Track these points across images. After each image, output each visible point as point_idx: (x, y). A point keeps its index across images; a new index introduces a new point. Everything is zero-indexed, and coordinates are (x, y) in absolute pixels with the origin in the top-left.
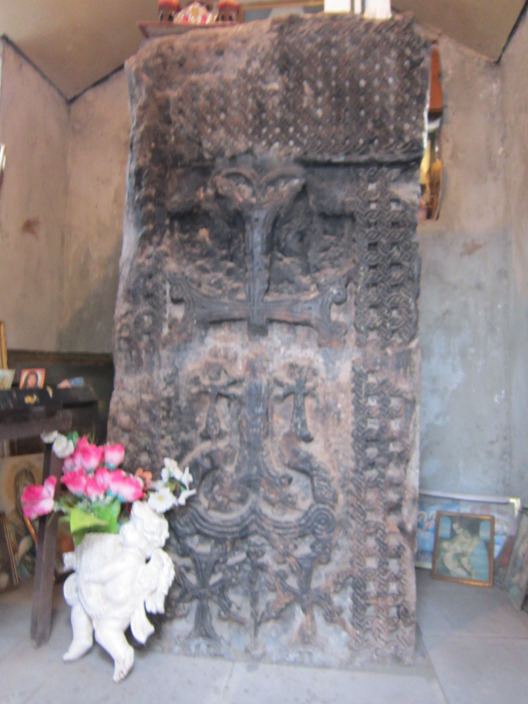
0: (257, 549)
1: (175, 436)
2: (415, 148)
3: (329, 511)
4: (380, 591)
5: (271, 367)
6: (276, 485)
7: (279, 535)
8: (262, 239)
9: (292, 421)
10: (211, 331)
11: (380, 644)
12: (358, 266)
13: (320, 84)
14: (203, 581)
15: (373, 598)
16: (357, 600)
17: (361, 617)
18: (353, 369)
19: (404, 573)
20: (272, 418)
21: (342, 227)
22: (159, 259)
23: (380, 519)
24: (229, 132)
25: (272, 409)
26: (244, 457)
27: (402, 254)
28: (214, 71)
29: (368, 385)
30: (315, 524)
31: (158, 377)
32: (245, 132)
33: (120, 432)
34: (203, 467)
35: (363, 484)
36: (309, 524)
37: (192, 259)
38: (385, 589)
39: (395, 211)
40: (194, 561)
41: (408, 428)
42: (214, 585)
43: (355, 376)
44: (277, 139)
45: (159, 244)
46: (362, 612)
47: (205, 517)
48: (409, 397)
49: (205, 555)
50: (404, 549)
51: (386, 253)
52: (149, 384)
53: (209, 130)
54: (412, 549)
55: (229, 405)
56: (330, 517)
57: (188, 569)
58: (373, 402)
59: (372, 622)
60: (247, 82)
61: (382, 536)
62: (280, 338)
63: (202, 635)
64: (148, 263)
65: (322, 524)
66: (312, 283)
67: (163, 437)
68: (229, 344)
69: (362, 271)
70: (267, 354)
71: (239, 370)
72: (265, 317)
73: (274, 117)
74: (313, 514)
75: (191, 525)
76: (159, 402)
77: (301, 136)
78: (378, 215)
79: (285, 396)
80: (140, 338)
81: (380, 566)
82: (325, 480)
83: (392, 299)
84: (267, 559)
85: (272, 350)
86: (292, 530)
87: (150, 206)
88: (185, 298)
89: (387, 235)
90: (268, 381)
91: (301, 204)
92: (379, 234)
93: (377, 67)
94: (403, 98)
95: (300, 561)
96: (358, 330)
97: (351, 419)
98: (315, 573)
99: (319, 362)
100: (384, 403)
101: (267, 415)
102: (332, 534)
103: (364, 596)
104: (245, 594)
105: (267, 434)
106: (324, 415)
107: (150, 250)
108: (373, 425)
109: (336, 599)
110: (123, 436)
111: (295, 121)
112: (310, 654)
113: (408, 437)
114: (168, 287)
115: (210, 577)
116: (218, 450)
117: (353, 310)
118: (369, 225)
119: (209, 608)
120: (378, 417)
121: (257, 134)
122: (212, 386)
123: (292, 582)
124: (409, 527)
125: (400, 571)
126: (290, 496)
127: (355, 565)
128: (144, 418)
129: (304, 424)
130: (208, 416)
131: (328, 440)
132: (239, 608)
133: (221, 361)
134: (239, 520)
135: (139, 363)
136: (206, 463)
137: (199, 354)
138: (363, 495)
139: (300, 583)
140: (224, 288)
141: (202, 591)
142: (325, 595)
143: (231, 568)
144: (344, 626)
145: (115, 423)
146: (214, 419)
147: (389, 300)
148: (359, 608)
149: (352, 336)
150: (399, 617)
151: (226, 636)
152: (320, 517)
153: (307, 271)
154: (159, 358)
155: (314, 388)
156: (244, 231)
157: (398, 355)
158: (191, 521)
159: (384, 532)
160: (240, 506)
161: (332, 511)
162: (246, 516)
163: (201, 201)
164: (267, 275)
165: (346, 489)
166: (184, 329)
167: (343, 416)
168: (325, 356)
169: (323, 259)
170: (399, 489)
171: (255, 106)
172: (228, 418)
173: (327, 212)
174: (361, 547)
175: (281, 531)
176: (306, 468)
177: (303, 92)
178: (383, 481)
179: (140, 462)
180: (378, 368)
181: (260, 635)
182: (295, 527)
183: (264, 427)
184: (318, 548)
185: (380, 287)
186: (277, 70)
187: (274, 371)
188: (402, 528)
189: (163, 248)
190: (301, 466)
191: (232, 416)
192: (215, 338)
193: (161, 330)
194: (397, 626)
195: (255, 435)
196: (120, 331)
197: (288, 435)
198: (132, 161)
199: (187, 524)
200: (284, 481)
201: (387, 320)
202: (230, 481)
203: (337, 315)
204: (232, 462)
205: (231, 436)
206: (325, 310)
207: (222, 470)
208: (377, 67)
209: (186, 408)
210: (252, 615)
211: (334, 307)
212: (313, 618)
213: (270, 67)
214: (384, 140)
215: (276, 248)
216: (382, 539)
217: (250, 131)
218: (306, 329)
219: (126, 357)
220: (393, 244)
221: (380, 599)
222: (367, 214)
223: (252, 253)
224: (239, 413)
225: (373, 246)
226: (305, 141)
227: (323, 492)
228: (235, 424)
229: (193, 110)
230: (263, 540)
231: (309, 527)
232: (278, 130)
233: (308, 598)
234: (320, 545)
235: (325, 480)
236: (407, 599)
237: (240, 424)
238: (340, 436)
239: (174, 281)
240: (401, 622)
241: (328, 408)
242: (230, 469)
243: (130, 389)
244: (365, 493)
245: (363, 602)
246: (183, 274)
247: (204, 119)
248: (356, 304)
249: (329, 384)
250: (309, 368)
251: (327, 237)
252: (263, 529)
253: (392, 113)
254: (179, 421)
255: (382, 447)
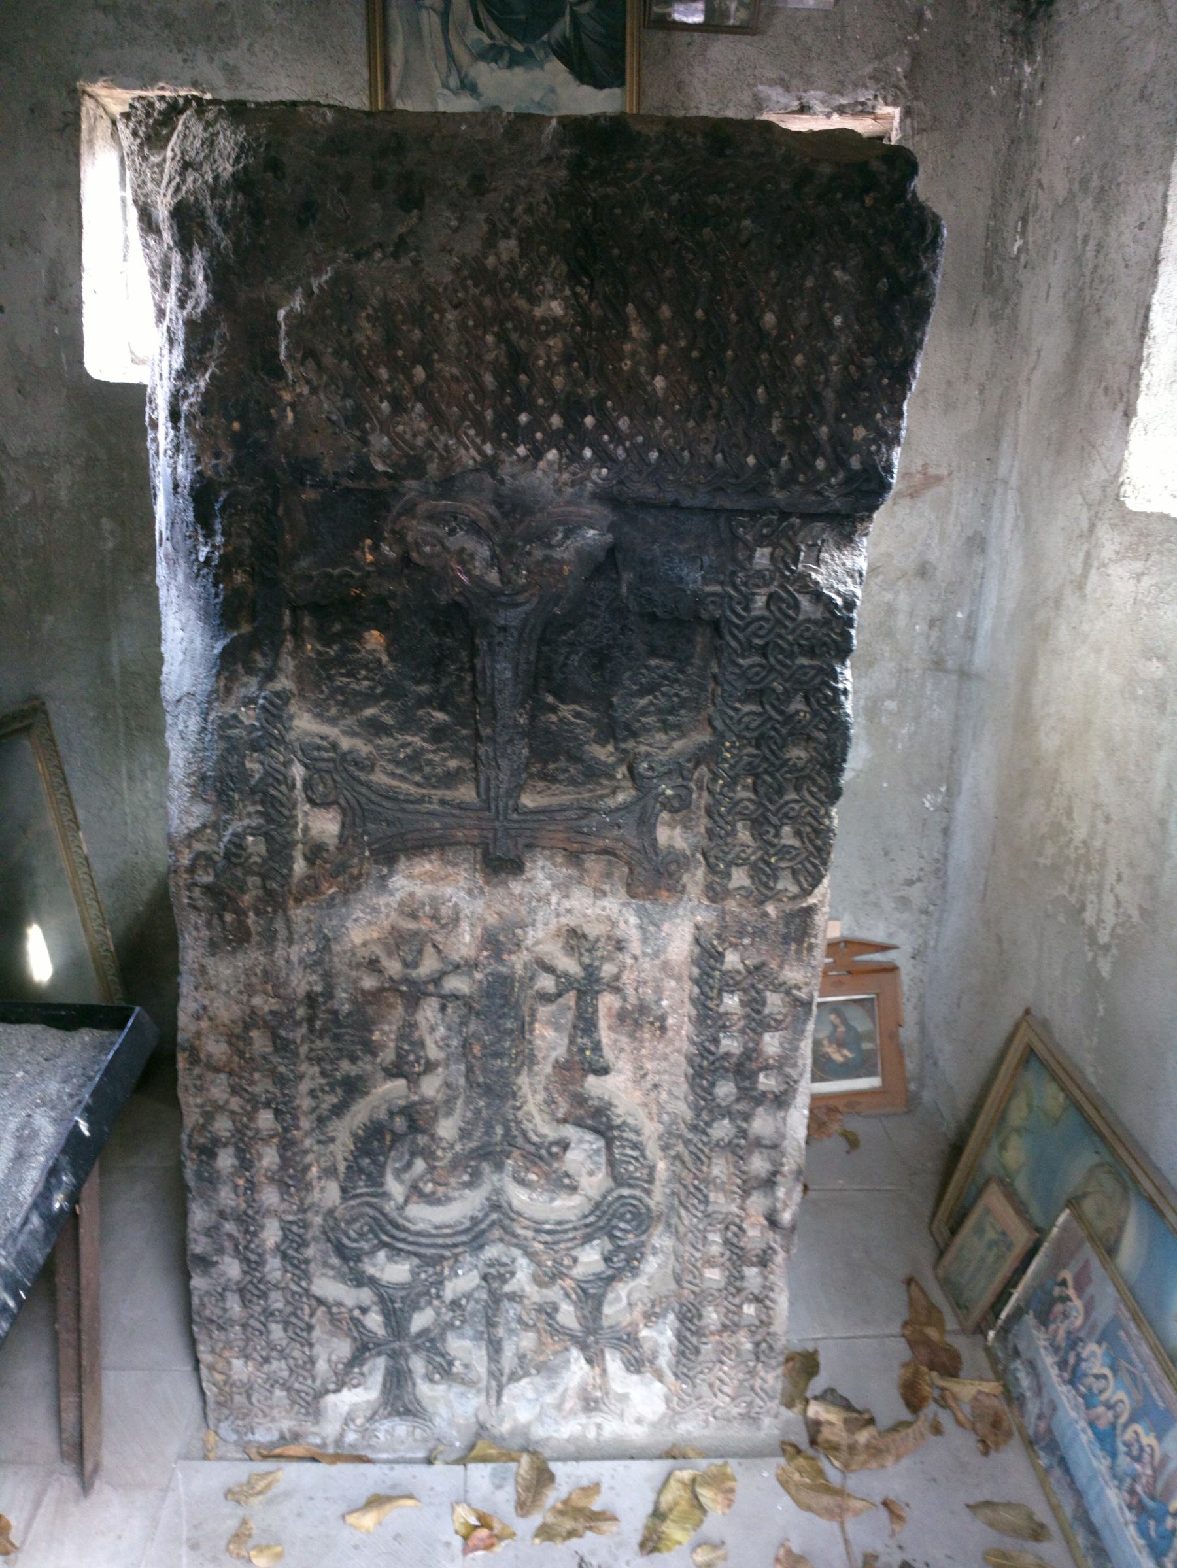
0: (502, 1270)
1: (328, 1067)
2: (873, 486)
3: (640, 1200)
4: (728, 1323)
5: (531, 936)
6: (541, 1158)
7: (545, 1243)
8: (516, 674)
9: (572, 1041)
10: (402, 864)
11: (722, 1401)
12: (720, 737)
13: (665, 312)
14: (396, 1320)
15: (712, 1333)
16: (685, 1338)
17: (691, 1364)
18: (697, 941)
19: (772, 1290)
20: (532, 1031)
21: (690, 641)
22: (275, 711)
23: (734, 1208)
24: (435, 416)
25: (533, 1015)
26: (478, 1112)
27: (815, 714)
28: (396, 255)
29: (724, 973)
30: (615, 1222)
31: (288, 961)
32: (478, 422)
33: (210, 1076)
34: (393, 1132)
35: (707, 1150)
36: (601, 1224)
37: (351, 702)
38: (736, 1318)
39: (808, 620)
40: (381, 1296)
41: (796, 1049)
42: (420, 1335)
43: (701, 956)
44: (555, 439)
45: (270, 676)
46: (693, 1357)
47: (400, 1221)
48: (803, 995)
49: (402, 1286)
50: (775, 1252)
51: (781, 713)
52: (267, 975)
53: (385, 406)
54: (787, 1251)
55: (443, 1008)
56: (643, 1210)
57: (364, 1311)
58: (731, 1002)
59: (711, 1369)
60: (482, 294)
61: (735, 1235)
62: (550, 877)
63: (399, 1414)
64: (249, 716)
65: (627, 1222)
66: (620, 761)
67: (301, 1077)
68: (437, 890)
69: (728, 750)
70: (524, 910)
71: (465, 943)
72: (522, 841)
73: (549, 391)
74: (610, 1205)
75: (371, 1236)
76: (292, 1011)
77: (611, 441)
78: (770, 631)
79: (559, 995)
80: (243, 889)
81: (729, 1283)
82: (635, 1146)
83: (785, 809)
84: (522, 1277)
85: (534, 903)
86: (570, 1235)
87: (239, 578)
88: (342, 801)
89: (787, 673)
90: (525, 967)
91: (601, 585)
92: (772, 669)
93: (809, 283)
94: (861, 368)
95: (584, 1285)
96: (711, 868)
97: (687, 1029)
98: (610, 1296)
99: (629, 924)
100: (755, 1004)
101: (523, 1030)
102: (644, 1238)
103: (699, 1333)
104: (478, 1337)
105: (523, 1064)
106: (636, 1021)
107: (250, 686)
108: (730, 1044)
109: (644, 1333)
110: (212, 1082)
111: (600, 400)
112: (599, 1426)
113: (795, 1065)
114: (298, 772)
115: (409, 1320)
116: (424, 1101)
117: (704, 821)
118: (748, 648)
119: (410, 1370)
120: (743, 1032)
121: (505, 430)
122: (407, 980)
123: (568, 1315)
124: (786, 1217)
125: (764, 1287)
126: (567, 1175)
127: (686, 1285)
128: (260, 1042)
129: (597, 1047)
130: (402, 1037)
131: (641, 1068)
132: (466, 1366)
133: (425, 925)
134: (468, 1224)
135: (240, 937)
136: (400, 1123)
137: (375, 910)
138: (704, 1169)
139: (582, 1319)
140: (427, 769)
141: (396, 1345)
142: (629, 1335)
143: (455, 1304)
144: (660, 1376)
145: (194, 1059)
146: (412, 1043)
147: (778, 810)
148: (686, 1350)
149: (698, 874)
150: (758, 1359)
151: (443, 1410)
152: (622, 1210)
153: (610, 732)
154: (288, 922)
155: (617, 978)
156: (473, 652)
157: (788, 918)
158: (371, 1230)
159: (740, 1228)
160: (467, 1191)
161: (646, 1199)
162: (480, 1215)
163: (369, 573)
164: (525, 752)
165: (673, 1153)
166: (340, 869)
167: (670, 1021)
168: (641, 912)
169: (644, 712)
170: (773, 1153)
171: (503, 358)
172: (442, 1031)
173: (659, 613)
174: (698, 1255)
175: (548, 1238)
176: (599, 1120)
177: (626, 336)
178: (743, 1142)
179: (257, 1131)
180: (746, 941)
181: (505, 1399)
182: (575, 1229)
183: (517, 1054)
184: (619, 1260)
185: (765, 782)
186: (564, 268)
187: (537, 943)
188: (772, 1221)
189: (284, 683)
190: (589, 1122)
191: (449, 1028)
192: (410, 877)
193: (291, 869)
194: (752, 1373)
195: (501, 1073)
196: (191, 870)
197: (561, 1067)
198: (177, 449)
199: (362, 1235)
200: (555, 1149)
201: (772, 851)
202: (449, 1155)
203: (670, 835)
204: (449, 1113)
205: (447, 1066)
206: (646, 824)
207: (433, 1137)
208: (809, 283)
209: (350, 1014)
210: (491, 1374)
211: (665, 815)
212: (604, 1372)
213: (545, 262)
214: (802, 463)
215: (543, 683)
216: (735, 1240)
217: (489, 415)
218: (607, 857)
219: (209, 925)
220: (796, 691)
221: (725, 1335)
222: (750, 624)
223: (492, 704)
224: (464, 1023)
225: (758, 695)
226: (620, 452)
227: (631, 1168)
228: (455, 1042)
229: (339, 353)
230: (516, 1252)
231: (602, 1228)
232: (556, 421)
233: (597, 1343)
234: (622, 1256)
235: (635, 1146)
236: (772, 1329)
237: (466, 1045)
238: (665, 1057)
239: (310, 754)
240: (760, 1366)
241: (643, 1009)
242: (447, 1129)
243: (224, 987)
244: (709, 1166)
245: (694, 1340)
246: (334, 746)
247: (373, 381)
248: (709, 813)
249: (646, 964)
250: (609, 938)
251: (653, 662)
252: (516, 1236)
253: (829, 394)
254: (336, 1038)
255: (747, 1084)
